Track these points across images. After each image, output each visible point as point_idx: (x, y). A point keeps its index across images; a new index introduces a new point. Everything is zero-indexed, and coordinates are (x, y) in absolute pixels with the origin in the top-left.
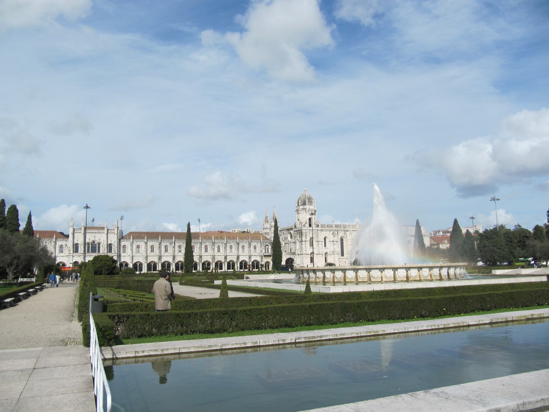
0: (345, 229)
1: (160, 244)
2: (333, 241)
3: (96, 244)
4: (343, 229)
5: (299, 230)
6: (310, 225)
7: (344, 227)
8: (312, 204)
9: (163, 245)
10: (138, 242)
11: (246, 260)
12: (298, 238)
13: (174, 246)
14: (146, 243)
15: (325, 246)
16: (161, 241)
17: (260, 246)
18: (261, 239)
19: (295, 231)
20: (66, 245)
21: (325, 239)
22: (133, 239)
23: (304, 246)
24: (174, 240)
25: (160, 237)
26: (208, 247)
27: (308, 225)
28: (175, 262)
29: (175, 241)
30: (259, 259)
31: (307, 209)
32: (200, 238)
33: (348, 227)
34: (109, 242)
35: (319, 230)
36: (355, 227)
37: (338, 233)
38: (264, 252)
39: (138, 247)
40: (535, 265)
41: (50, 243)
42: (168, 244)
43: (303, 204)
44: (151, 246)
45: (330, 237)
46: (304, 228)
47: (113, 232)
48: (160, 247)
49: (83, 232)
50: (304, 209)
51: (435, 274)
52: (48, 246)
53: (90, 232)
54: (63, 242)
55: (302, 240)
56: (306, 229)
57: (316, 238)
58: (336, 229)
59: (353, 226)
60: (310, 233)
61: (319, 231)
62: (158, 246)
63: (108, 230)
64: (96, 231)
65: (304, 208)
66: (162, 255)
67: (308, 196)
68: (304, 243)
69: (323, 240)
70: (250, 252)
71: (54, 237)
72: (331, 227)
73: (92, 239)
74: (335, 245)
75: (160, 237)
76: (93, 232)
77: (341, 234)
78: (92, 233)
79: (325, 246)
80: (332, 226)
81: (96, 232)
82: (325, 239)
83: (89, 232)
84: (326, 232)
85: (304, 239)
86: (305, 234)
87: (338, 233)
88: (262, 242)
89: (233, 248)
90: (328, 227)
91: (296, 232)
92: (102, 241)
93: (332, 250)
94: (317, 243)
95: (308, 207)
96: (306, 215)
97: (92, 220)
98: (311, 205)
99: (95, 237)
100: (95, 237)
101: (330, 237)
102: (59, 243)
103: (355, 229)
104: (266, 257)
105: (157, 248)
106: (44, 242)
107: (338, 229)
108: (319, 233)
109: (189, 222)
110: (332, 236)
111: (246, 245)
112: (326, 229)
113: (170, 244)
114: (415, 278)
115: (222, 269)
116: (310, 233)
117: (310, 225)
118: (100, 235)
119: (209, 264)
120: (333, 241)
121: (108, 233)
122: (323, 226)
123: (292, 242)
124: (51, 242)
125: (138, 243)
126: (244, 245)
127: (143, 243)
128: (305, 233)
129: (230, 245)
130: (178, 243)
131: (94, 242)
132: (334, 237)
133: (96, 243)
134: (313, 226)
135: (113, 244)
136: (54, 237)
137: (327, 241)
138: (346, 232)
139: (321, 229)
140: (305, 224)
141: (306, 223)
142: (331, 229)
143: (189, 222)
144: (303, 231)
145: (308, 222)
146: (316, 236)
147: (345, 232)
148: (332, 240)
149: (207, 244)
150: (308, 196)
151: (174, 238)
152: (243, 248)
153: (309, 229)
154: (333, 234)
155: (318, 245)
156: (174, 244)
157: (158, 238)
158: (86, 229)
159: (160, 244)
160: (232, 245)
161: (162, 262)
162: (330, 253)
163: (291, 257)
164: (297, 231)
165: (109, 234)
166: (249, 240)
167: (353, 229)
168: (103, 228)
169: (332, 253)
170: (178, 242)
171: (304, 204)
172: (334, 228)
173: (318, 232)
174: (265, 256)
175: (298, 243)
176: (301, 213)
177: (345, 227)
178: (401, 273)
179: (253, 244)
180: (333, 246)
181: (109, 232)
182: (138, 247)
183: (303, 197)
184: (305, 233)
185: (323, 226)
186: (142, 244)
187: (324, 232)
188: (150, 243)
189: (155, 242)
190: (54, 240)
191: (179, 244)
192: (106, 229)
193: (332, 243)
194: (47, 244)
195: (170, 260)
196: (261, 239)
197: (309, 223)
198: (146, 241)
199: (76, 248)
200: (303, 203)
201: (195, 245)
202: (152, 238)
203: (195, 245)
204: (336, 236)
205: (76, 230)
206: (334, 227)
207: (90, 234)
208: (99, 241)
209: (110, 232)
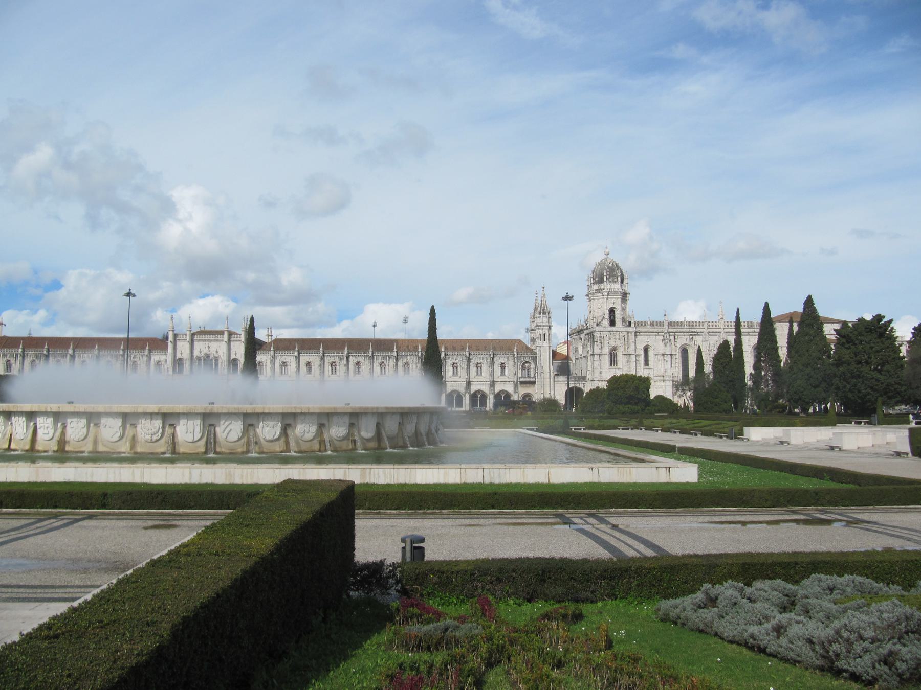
0: (693, 330)
1: (322, 359)
2: (663, 355)
3: (212, 360)
4: (688, 330)
5: (590, 333)
6: (612, 323)
7: (689, 325)
8: (617, 280)
9: (328, 360)
10: (284, 357)
11: (484, 390)
12: (589, 349)
13: (345, 362)
14: (298, 359)
15: (647, 363)
16: (323, 354)
17: (512, 363)
18: (515, 350)
19: (586, 335)
20: (166, 361)
21: (646, 350)
22: (274, 351)
23: (596, 364)
24: (346, 353)
25: (321, 348)
26: (411, 365)
27: (606, 322)
28: (494, 393)
29: (348, 354)
30: (510, 388)
31: (605, 290)
32: (395, 350)
33: (699, 325)
34: (233, 357)
35: (631, 332)
36: (716, 326)
37: (675, 337)
38: (520, 375)
39: (284, 364)
40: (911, 417)
41: (141, 358)
42: (337, 360)
43: (599, 280)
44: (308, 364)
45: (657, 345)
46: (598, 329)
47: (238, 339)
48: (322, 365)
49: (188, 338)
50: (600, 291)
51: (149, 437)
52: (138, 363)
53: (201, 339)
54: (161, 356)
55: (593, 352)
56: (602, 330)
57: (625, 349)
58: (670, 330)
59: (711, 324)
60: (610, 339)
61: (630, 334)
62: (319, 363)
63: (231, 334)
64: (211, 337)
65: (601, 289)
66: (471, 380)
67: (611, 265)
68: (596, 357)
69: (642, 353)
70: (492, 375)
71: (147, 348)
72: (660, 325)
73: (205, 351)
74: (667, 361)
75: (321, 348)
76: (206, 339)
77: (682, 340)
78: (205, 340)
79: (647, 363)
80: (661, 324)
81: (211, 339)
82: (646, 350)
83: (200, 339)
84: (647, 337)
85: (597, 351)
86: (600, 340)
87: (675, 337)
88: (516, 356)
89: (459, 368)
90: (653, 325)
91: (587, 336)
92: (220, 353)
93: (662, 372)
94: (625, 358)
95: (608, 287)
96: (603, 303)
97: (373, 324)
98: (615, 282)
99: (209, 347)
100: (209, 347)
101: (657, 345)
102: (155, 357)
103: (717, 330)
104: (525, 385)
105: (317, 366)
106: (133, 356)
107: (675, 330)
108: (630, 338)
109: (252, 316)
110: (662, 344)
111: (485, 362)
112: (647, 330)
113: (341, 360)
114: (81, 447)
115: (461, 406)
116: (610, 339)
117: (612, 323)
118: (218, 343)
119: (484, 396)
120: (663, 355)
121: (229, 340)
122: (642, 325)
123: (582, 356)
124: (142, 356)
125: (283, 359)
126: (482, 361)
127: (292, 357)
128: (598, 338)
129: (454, 361)
130: (354, 358)
131: (207, 356)
132: (665, 346)
133: (211, 358)
134: (618, 322)
135: (239, 359)
136: (147, 348)
137: (651, 354)
138: (694, 337)
139: (638, 330)
140: (602, 320)
141: (604, 318)
142: (659, 330)
143: (252, 316)
144: (595, 334)
145: (607, 316)
146: (625, 344)
147: (691, 335)
148: (661, 352)
149: (409, 359)
150: (611, 265)
151: (346, 349)
152: (479, 368)
153: (608, 330)
154: (663, 340)
155: (628, 362)
156: (345, 359)
157: (294, 349)
158: (193, 335)
159: (322, 359)
160: (457, 361)
161: (472, 393)
162: (656, 378)
163: (578, 385)
164: (588, 334)
165: (232, 343)
166: (491, 353)
167: (709, 330)
168: (222, 333)
169: (661, 378)
170: (355, 356)
171: (601, 281)
172: (666, 329)
173: (628, 336)
174: (522, 383)
175: (589, 358)
176: (594, 299)
177: (693, 325)
178: (46, 428)
179: (499, 360)
180: (662, 364)
181: (232, 339)
182: (284, 364)
183: (599, 267)
184: (598, 338)
185: (638, 324)
186: (291, 359)
187: (644, 335)
188: (305, 358)
189: (313, 357)
190: (146, 352)
191: (356, 360)
192: (226, 334)
193: (662, 359)
194: (137, 359)
195: (485, 388)
196: (515, 350)
197: (610, 318)
198: (296, 354)
199: (178, 363)
200: (599, 278)
201: (385, 361)
202: (310, 349)
203: (385, 361)
204: (669, 344)
205: (179, 336)
206: (666, 326)
207: (201, 342)
208: (216, 355)
209: (234, 339)
